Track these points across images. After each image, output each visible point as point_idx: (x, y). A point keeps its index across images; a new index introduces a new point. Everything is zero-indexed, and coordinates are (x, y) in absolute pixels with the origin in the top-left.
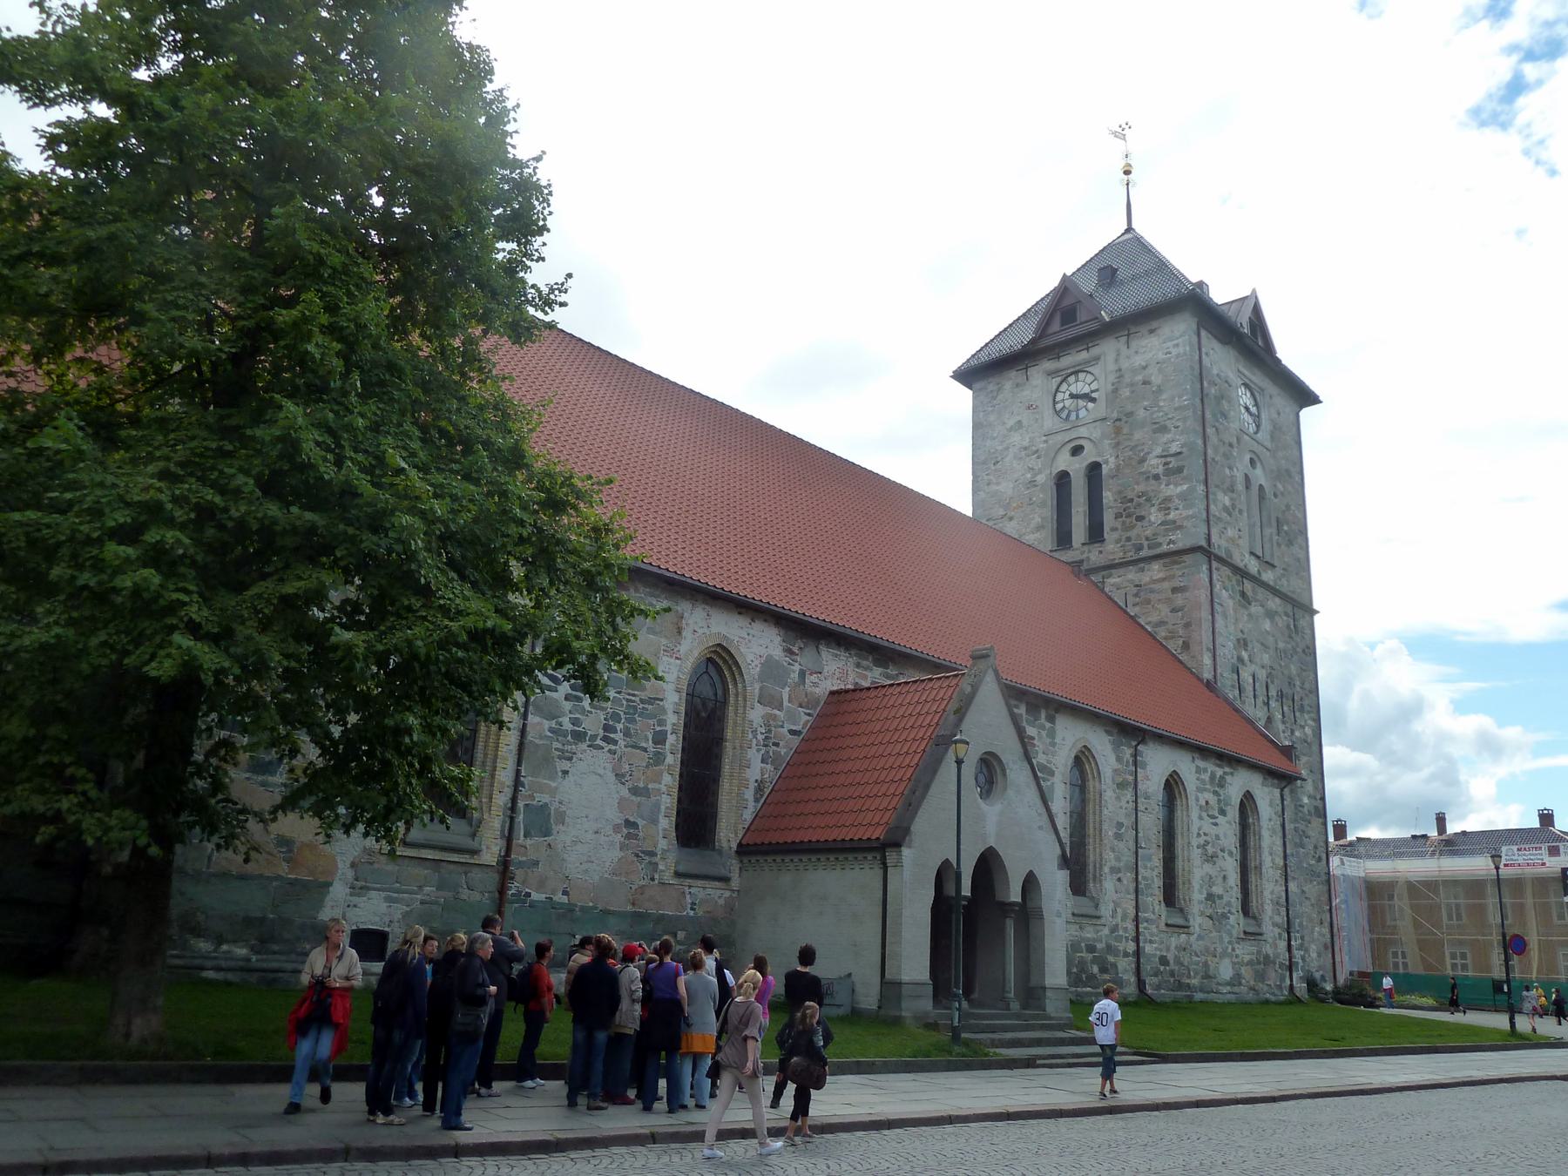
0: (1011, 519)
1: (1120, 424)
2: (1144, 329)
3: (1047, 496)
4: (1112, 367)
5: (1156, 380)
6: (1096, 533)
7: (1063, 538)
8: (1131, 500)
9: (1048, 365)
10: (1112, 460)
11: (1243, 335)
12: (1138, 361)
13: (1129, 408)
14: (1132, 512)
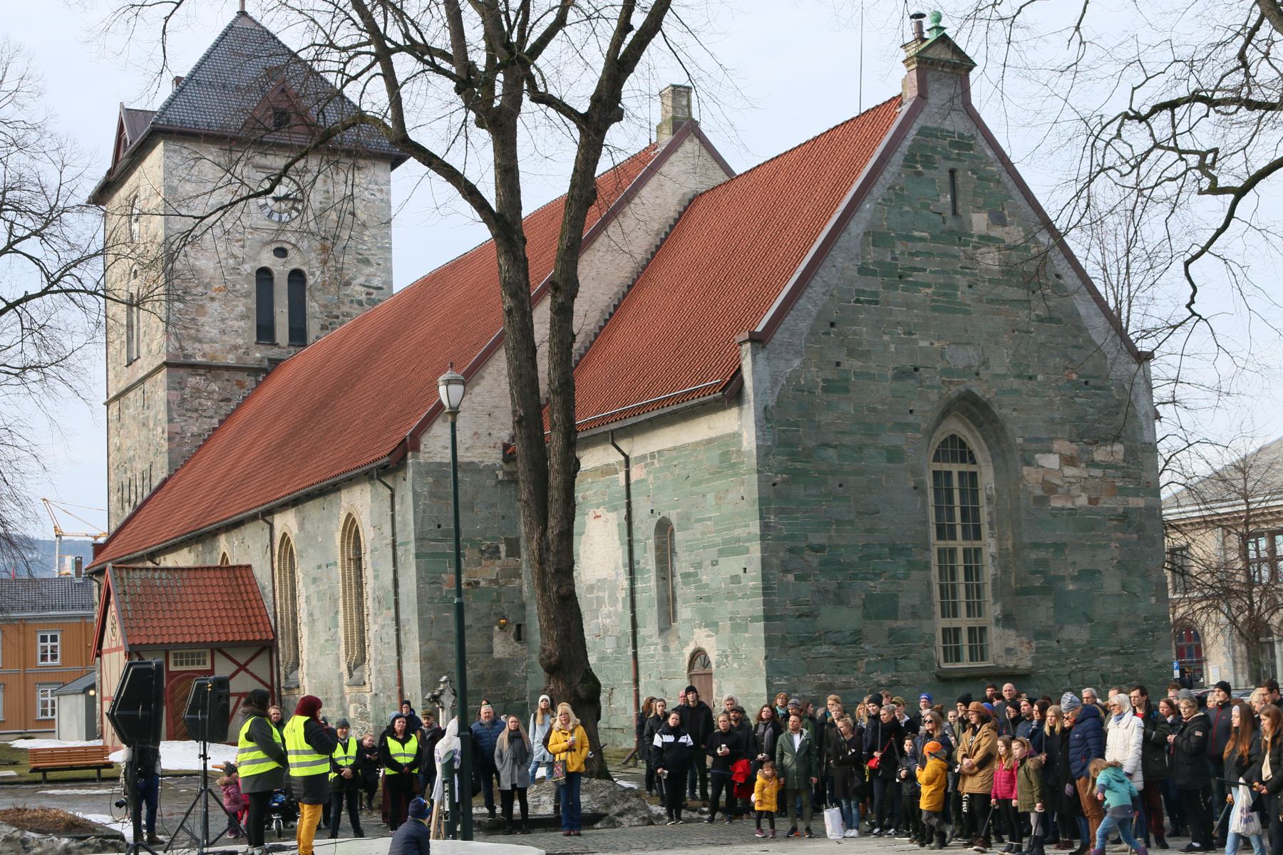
0: (212, 299)
3: (249, 286)
5: (362, 216)
8: (337, 317)
10: (318, 273)
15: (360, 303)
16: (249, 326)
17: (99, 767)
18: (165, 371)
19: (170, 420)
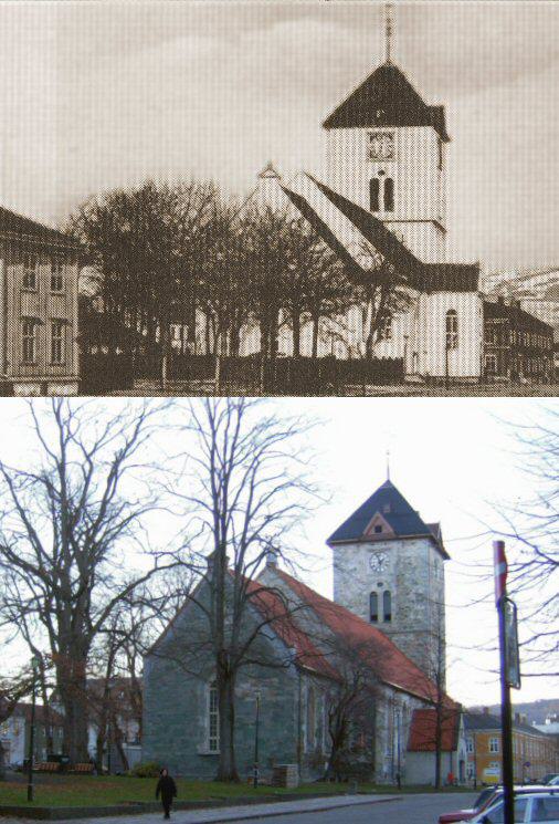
1: (399, 579)
2: (410, 542)
4: (395, 553)
6: (388, 618)
7: (374, 618)
9: (367, 546)
11: (432, 535)
12: (408, 554)
14: (403, 612)
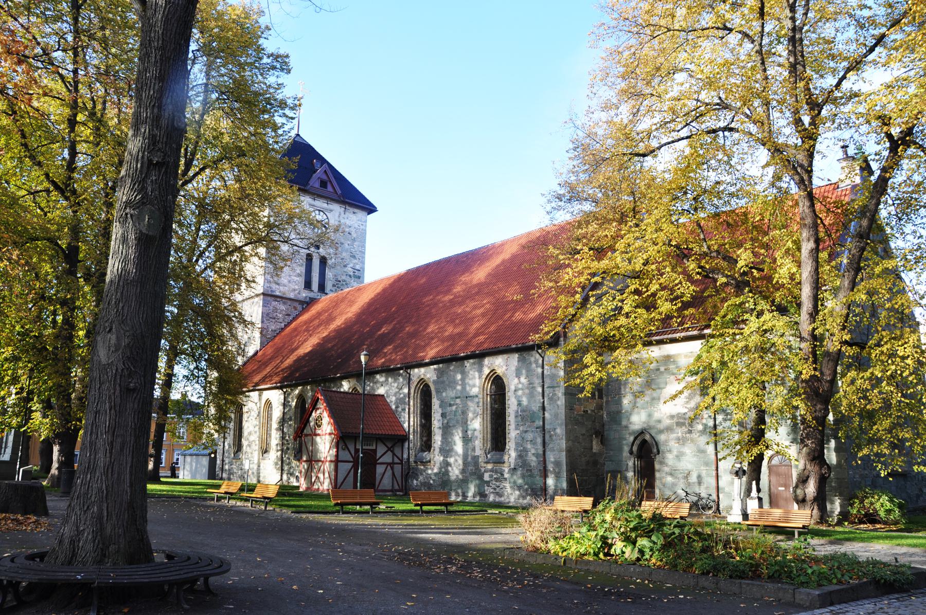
2: (352, 210)
5: (354, 235)
12: (348, 222)
13: (343, 241)
15: (350, 276)
16: (301, 280)
17: (446, 505)
18: (262, 297)
19: (262, 322)
